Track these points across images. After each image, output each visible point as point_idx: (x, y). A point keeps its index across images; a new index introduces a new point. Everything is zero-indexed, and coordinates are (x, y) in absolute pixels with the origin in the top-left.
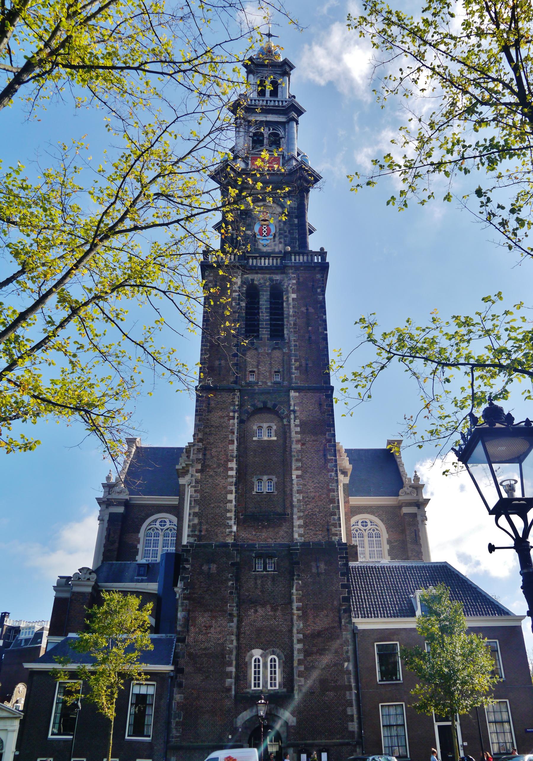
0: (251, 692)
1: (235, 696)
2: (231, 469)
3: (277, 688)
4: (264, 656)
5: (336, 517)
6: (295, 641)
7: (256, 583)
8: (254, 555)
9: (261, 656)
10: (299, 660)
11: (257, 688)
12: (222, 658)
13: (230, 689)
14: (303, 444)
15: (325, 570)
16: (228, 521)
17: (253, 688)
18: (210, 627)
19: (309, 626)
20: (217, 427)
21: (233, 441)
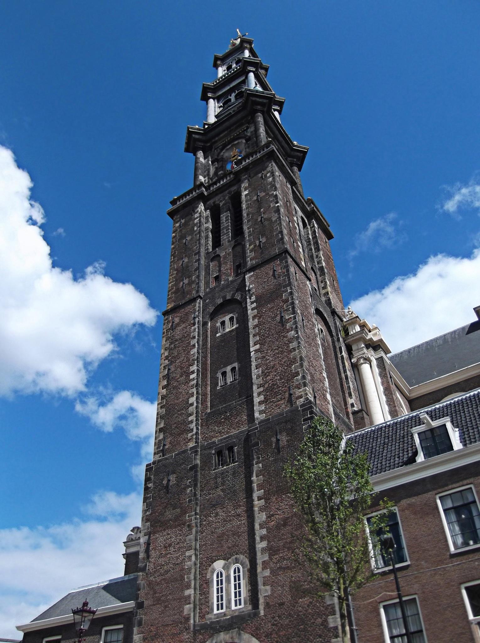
0: (213, 617)
1: (194, 625)
2: (193, 372)
3: (242, 606)
4: (226, 567)
5: (300, 377)
6: (258, 538)
7: (216, 483)
8: (213, 452)
9: (223, 568)
10: (264, 562)
11: (220, 611)
12: (181, 580)
13: (188, 619)
14: (260, 317)
15: (288, 441)
16: (190, 425)
17: (215, 612)
18: (170, 545)
19: (273, 515)
20: (180, 339)
21: (194, 346)
